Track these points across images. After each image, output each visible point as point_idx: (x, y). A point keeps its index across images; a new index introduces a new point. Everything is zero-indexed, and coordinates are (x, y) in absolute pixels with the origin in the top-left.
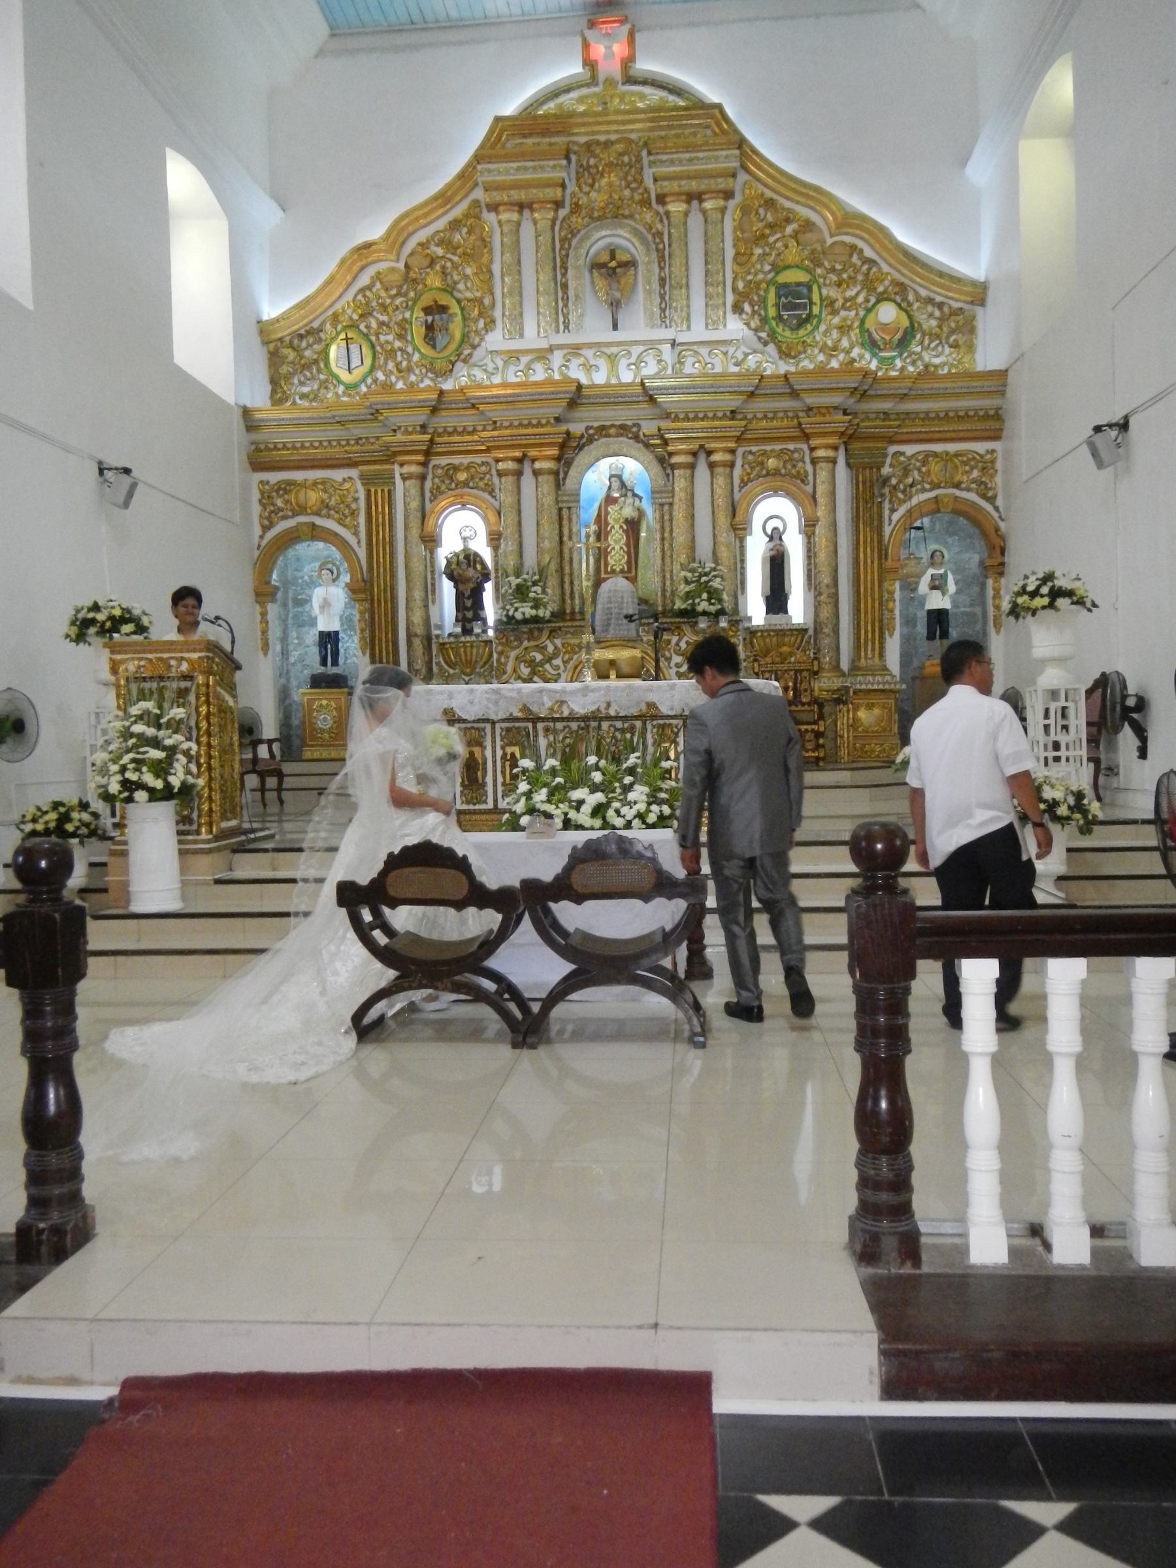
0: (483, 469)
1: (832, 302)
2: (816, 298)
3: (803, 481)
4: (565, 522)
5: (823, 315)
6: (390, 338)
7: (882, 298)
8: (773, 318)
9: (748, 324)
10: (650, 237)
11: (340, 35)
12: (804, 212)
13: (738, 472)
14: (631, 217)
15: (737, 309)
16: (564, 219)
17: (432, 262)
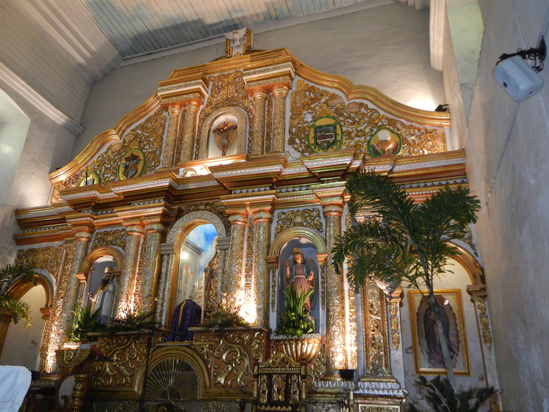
0: (122, 233)
1: (349, 134)
2: (339, 131)
3: (318, 229)
4: (165, 264)
5: (344, 141)
6: (109, 175)
7: (379, 128)
8: (312, 144)
9: (296, 149)
10: (246, 113)
11: (127, 59)
12: (332, 91)
13: (274, 226)
14: (237, 105)
15: (292, 142)
16: (203, 110)
17: (136, 136)
